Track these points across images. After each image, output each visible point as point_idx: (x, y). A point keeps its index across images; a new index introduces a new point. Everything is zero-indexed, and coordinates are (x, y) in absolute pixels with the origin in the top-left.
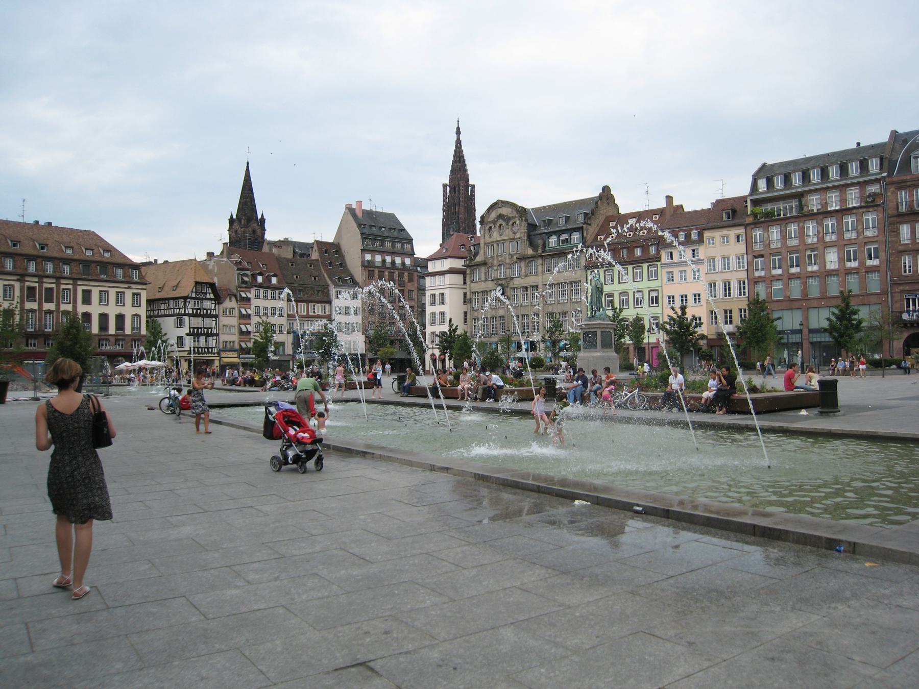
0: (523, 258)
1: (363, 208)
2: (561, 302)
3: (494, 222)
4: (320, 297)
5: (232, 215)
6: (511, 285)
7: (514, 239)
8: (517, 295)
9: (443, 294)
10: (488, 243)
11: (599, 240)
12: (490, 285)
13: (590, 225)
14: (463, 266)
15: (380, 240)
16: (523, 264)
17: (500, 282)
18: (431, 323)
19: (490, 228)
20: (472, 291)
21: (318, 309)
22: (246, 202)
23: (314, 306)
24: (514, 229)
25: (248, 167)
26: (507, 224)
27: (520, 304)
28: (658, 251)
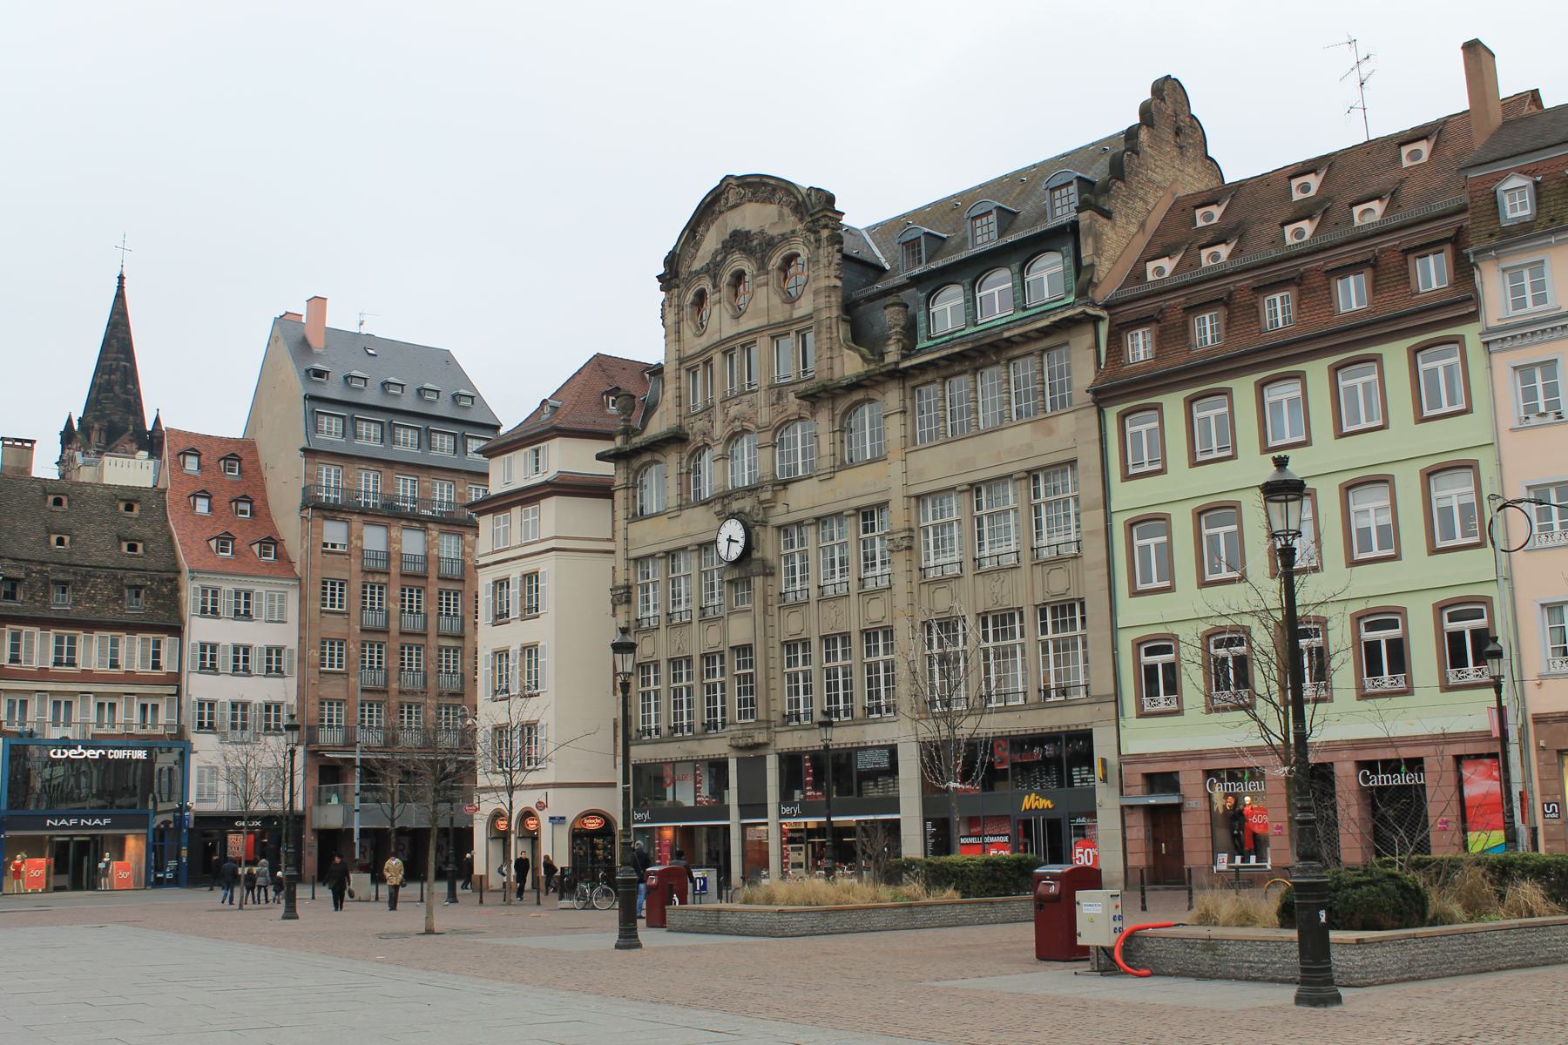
0: (819, 396)
1: (331, 322)
2: (987, 565)
3: (713, 270)
4: (135, 608)
5: (70, 420)
6: (779, 516)
7: (789, 322)
8: (804, 558)
9: (530, 578)
10: (692, 357)
11: (1150, 277)
12: (697, 522)
13: (1108, 215)
14: (601, 457)
15: (381, 423)
16: (823, 422)
17: (736, 506)
18: (496, 692)
19: (701, 297)
20: (633, 554)
21: (133, 651)
22: (109, 382)
23: (115, 643)
24: (792, 282)
25: (121, 287)
26: (762, 267)
27: (814, 593)
28: (1464, 270)
